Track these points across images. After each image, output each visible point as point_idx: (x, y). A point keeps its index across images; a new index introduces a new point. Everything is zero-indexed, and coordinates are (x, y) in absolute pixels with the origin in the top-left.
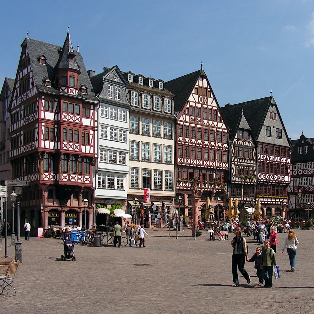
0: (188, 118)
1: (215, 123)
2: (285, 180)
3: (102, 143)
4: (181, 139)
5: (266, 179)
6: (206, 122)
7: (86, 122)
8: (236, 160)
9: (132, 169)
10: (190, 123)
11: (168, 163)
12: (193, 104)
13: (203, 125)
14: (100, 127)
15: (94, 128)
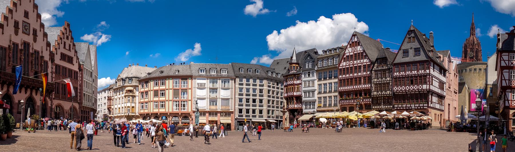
0: (344, 64)
1: (362, 61)
2: (422, 89)
3: (303, 89)
4: (340, 76)
5: (401, 90)
6: (355, 62)
7: (298, 82)
8: (375, 80)
9: (319, 98)
10: (346, 66)
11: (335, 91)
12: (348, 54)
13: (353, 65)
14: (303, 83)
15: (301, 84)
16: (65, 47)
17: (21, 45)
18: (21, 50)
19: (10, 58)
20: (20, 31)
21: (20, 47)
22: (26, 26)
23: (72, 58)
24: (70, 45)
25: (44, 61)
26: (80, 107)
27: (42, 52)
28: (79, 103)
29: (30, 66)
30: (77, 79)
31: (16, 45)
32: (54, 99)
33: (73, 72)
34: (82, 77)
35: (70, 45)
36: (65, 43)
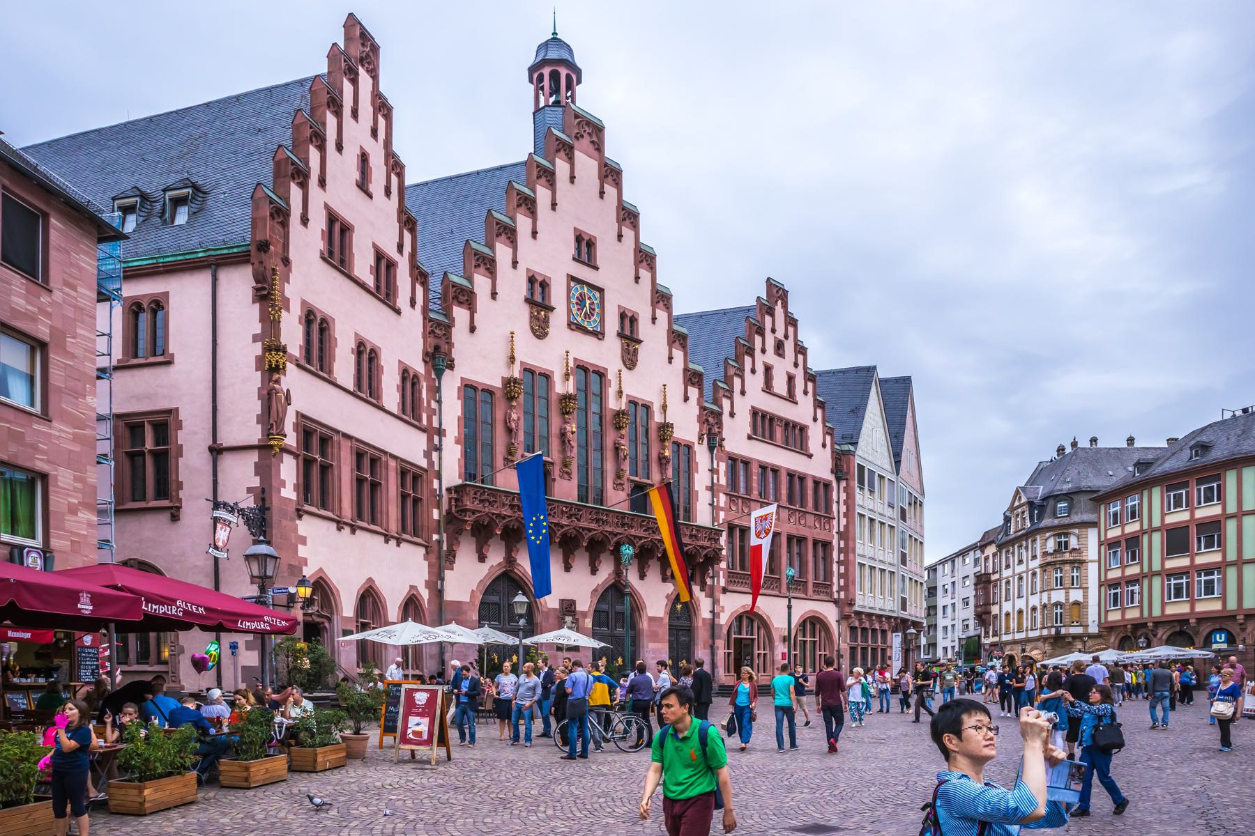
16: (768, 388)
17: (567, 376)
18: (566, 398)
19: (509, 431)
20: (558, 319)
21: (560, 387)
22: (588, 298)
23: (803, 429)
24: (791, 378)
25: (677, 444)
26: (844, 617)
27: (664, 407)
28: (836, 602)
29: (610, 467)
30: (828, 508)
31: (537, 377)
32: (725, 590)
33: (810, 485)
34: (850, 502)
35: (791, 378)
36: (768, 369)
